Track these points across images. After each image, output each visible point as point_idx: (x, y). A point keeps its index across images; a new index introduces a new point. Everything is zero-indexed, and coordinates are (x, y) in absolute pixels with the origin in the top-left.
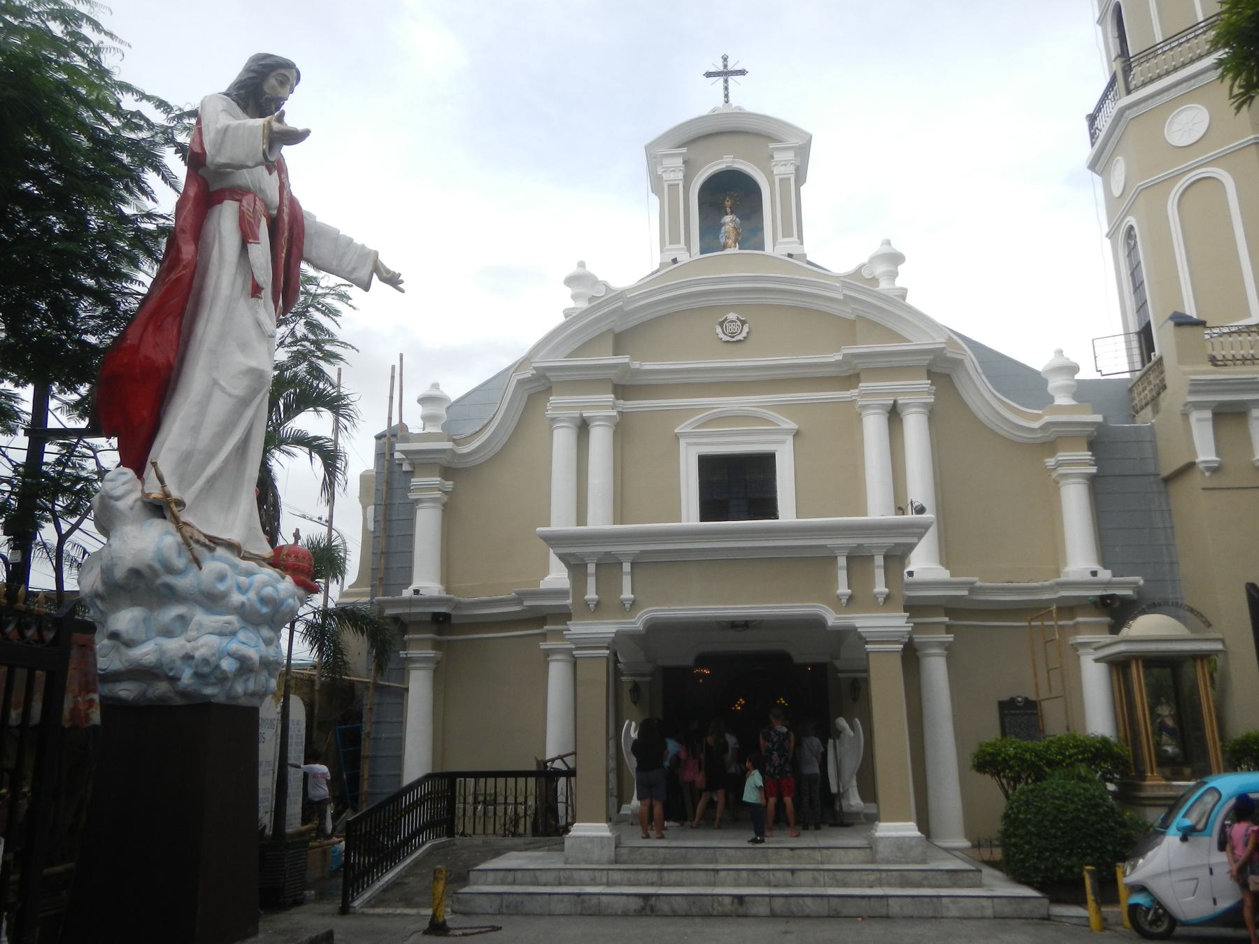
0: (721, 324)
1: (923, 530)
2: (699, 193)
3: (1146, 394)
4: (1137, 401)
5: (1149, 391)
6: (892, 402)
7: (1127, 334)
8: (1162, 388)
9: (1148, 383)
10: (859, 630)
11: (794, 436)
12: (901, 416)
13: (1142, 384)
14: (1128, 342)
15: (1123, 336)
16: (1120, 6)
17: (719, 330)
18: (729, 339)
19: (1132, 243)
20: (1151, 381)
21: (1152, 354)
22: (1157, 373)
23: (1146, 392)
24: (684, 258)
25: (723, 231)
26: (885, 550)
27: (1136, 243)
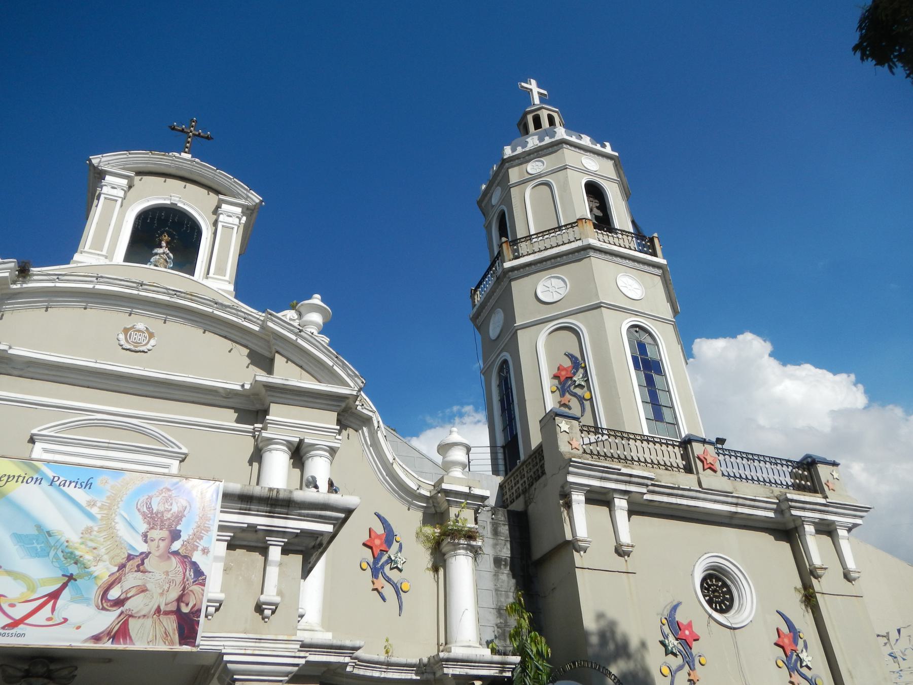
0: (126, 331)
1: (343, 515)
3: (519, 488)
4: (508, 496)
5: (522, 485)
6: (297, 440)
7: (493, 446)
8: (536, 478)
9: (521, 478)
10: (226, 658)
11: (181, 462)
12: (304, 458)
13: (515, 479)
15: (489, 448)
17: (122, 337)
18: (132, 347)
20: (524, 475)
21: (518, 461)
22: (531, 466)
23: (519, 485)
24: (103, 261)
25: (152, 260)
26: (286, 540)
27: (508, 372)
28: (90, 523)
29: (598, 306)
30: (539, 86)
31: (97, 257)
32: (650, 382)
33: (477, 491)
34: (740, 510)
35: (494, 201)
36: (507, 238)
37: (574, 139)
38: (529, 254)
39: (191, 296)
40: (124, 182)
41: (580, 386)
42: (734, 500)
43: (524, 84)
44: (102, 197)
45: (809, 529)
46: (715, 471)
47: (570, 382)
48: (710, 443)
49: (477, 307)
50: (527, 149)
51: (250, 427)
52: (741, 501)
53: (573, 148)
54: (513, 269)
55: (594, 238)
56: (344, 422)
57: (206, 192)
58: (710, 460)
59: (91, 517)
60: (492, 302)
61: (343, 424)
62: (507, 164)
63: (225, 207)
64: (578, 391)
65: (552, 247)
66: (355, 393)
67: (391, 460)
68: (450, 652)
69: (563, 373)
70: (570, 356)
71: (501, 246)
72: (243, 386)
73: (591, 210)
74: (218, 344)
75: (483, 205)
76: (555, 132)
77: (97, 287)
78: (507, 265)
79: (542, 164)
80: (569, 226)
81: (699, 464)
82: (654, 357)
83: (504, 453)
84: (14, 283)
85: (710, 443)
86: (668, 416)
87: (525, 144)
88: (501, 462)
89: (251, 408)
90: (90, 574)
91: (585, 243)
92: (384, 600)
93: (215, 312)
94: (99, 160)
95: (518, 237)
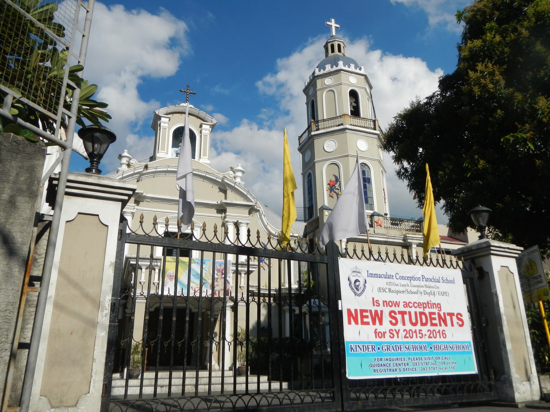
2: (174, 132)
4: (308, 231)
7: (305, 208)
14: (305, 210)
16: (314, 101)
19: (310, 178)
23: (311, 228)
27: (311, 178)
28: (206, 272)
29: (347, 156)
30: (336, 23)
31: (163, 153)
32: (365, 187)
33: (295, 235)
34: (389, 240)
35: (311, 93)
36: (314, 120)
37: (346, 68)
38: (322, 129)
39: (198, 170)
40: (168, 119)
41: (337, 189)
42: (387, 237)
43: (328, 23)
44: (161, 127)
45: (414, 246)
46: (381, 227)
47: (334, 187)
48: (382, 216)
49: (301, 145)
50: (325, 72)
51: (220, 215)
52: (389, 237)
53: (345, 73)
54: (315, 135)
55: (349, 122)
56: (251, 212)
57: (196, 118)
58: (380, 223)
59: (206, 270)
60: (306, 146)
61: (250, 213)
62: (316, 78)
63: (203, 126)
64: (337, 191)
65: (331, 127)
66: (254, 204)
67: (266, 224)
68: (285, 286)
69: (332, 183)
70: (335, 176)
71: (311, 123)
72: (217, 202)
73: (351, 104)
74: (208, 185)
75: (306, 92)
76: (338, 64)
77: (169, 169)
78: (313, 133)
79: (331, 80)
80: (339, 117)
81: (376, 224)
82: (368, 177)
83: (309, 210)
84: (144, 171)
85: (382, 216)
86: (370, 202)
87: (324, 69)
88: (307, 214)
89: (220, 209)
90: (208, 282)
91: (345, 127)
92: (264, 270)
93: (206, 175)
94: (158, 112)
95: (319, 120)
